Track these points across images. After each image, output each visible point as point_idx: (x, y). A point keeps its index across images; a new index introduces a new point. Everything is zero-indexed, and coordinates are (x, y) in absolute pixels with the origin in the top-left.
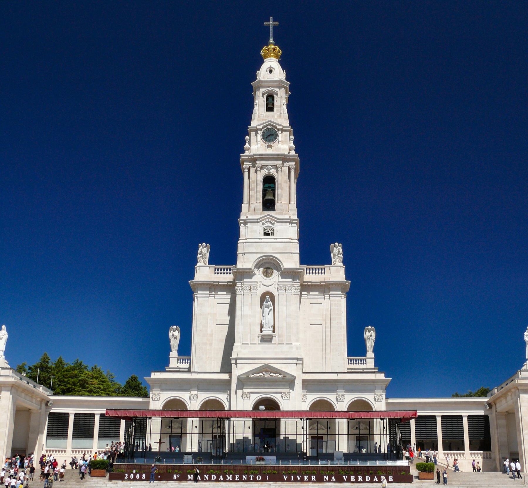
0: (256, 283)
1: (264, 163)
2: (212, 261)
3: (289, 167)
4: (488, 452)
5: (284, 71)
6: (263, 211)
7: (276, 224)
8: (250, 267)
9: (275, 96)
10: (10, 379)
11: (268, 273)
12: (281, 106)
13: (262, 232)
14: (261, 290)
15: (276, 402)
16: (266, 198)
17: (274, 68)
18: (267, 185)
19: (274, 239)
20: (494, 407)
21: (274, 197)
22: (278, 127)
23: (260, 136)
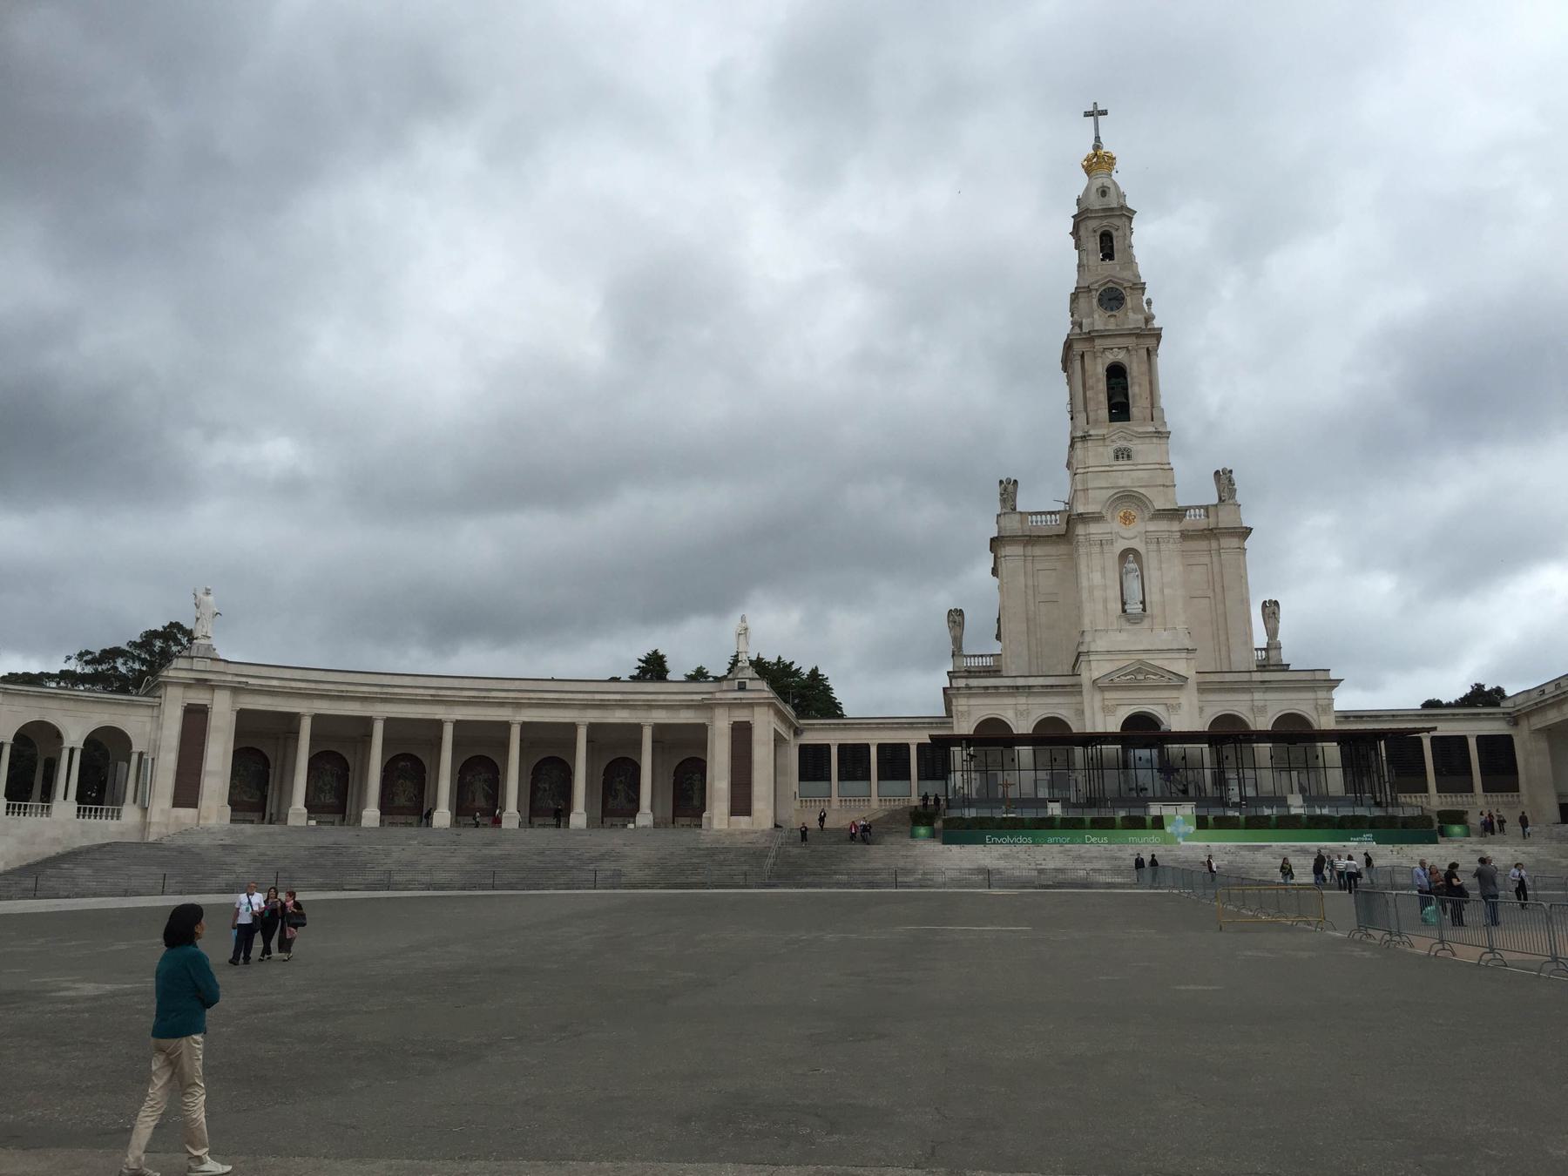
0: (1110, 535)
1: (1108, 343)
4: (1516, 794)
6: (1110, 421)
7: (1136, 441)
9: (1115, 234)
10: (765, 695)
11: (1127, 519)
13: (1112, 455)
14: (1121, 546)
15: (1142, 716)
16: (1112, 402)
17: (1109, 188)
18: (1113, 380)
19: (1133, 465)
21: (1127, 399)
22: (1125, 285)
23: (1095, 301)
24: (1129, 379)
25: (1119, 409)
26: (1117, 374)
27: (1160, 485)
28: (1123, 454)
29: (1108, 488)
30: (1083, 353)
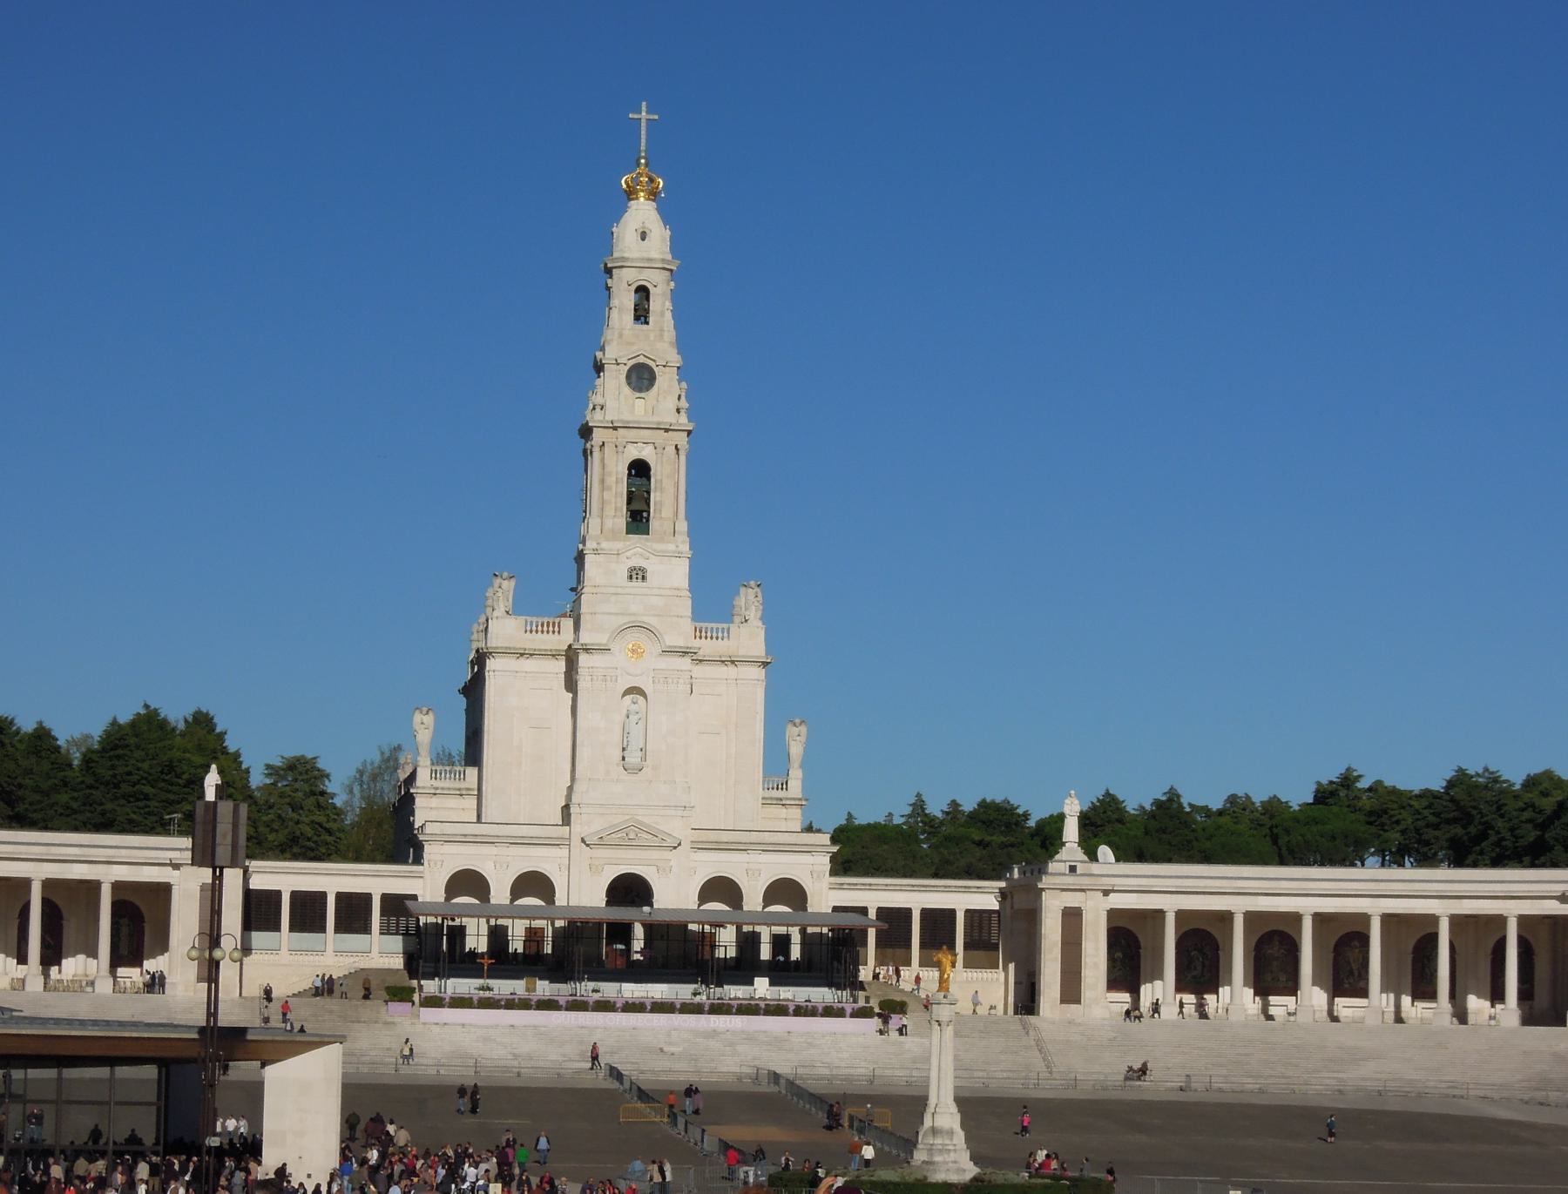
1: (632, 435)
2: (517, 610)
3: (676, 446)
5: (668, 227)
6: (627, 533)
8: (604, 641)
12: (662, 314)
13: (626, 574)
20: (1009, 899)
24: (652, 480)
25: (638, 519)
26: (640, 469)
27: (674, 616)
28: (638, 574)
29: (617, 614)
30: (603, 443)
